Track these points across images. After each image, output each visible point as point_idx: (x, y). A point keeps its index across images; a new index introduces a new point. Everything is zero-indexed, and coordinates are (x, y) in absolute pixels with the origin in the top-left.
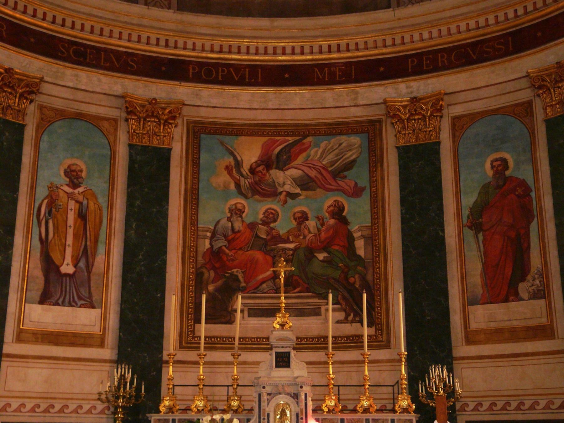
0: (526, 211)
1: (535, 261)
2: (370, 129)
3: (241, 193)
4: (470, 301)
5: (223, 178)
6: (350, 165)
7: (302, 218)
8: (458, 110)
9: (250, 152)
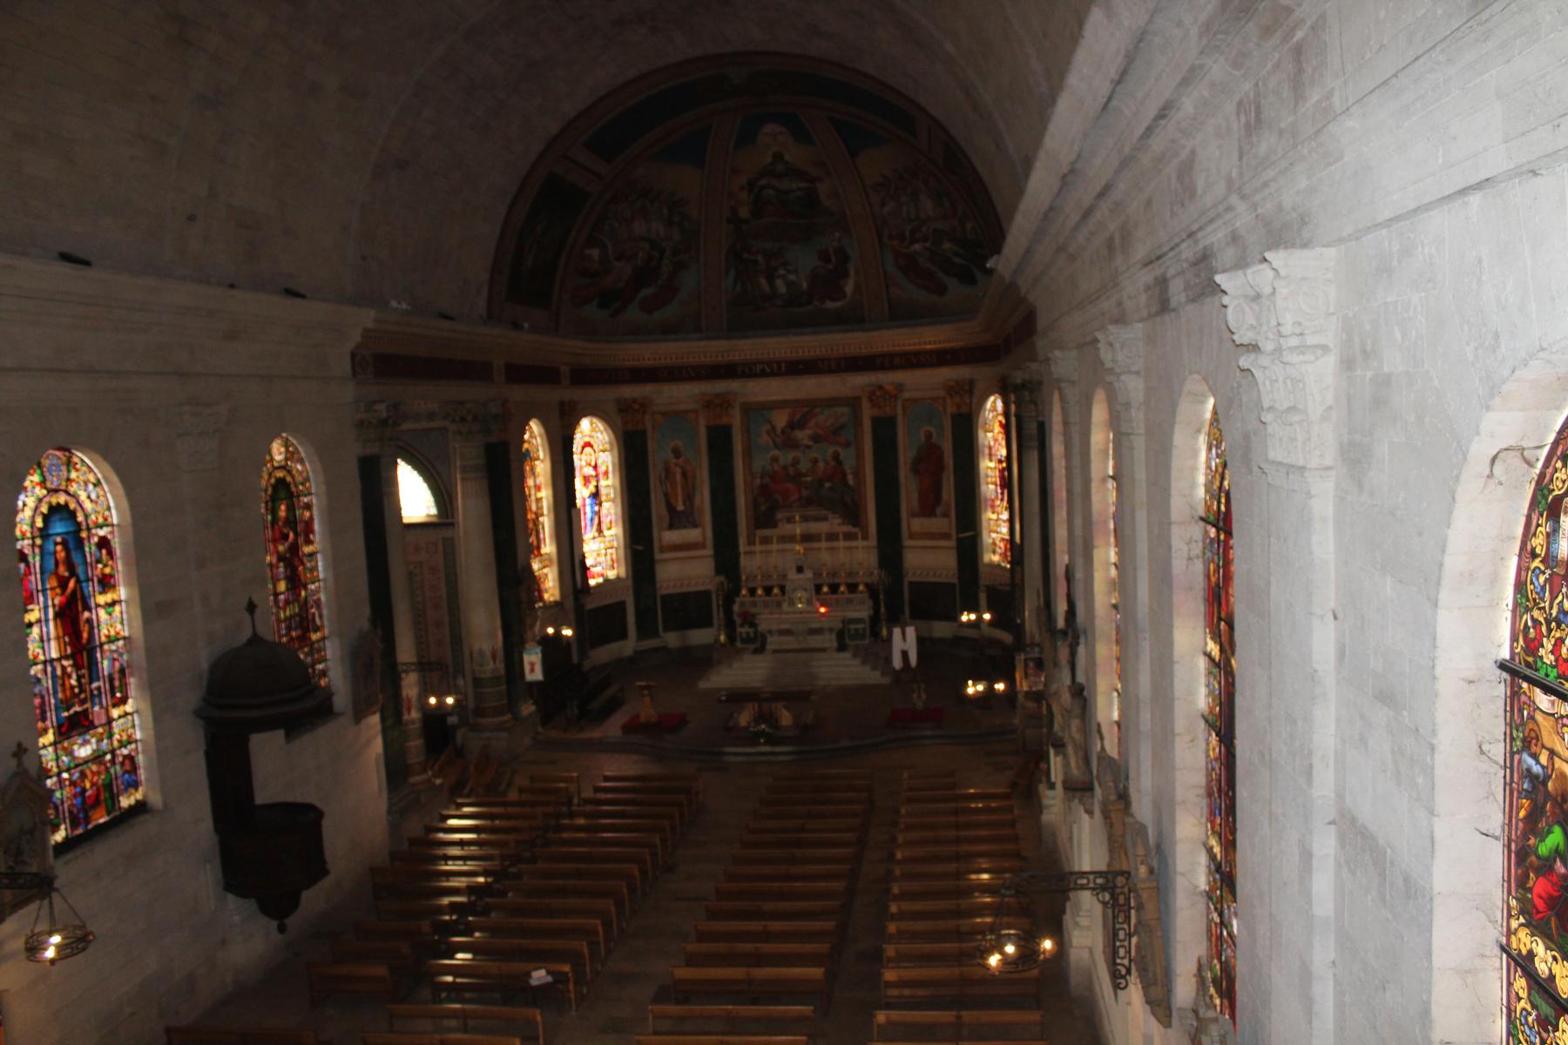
0: (941, 467)
1: (945, 496)
2: (853, 403)
3: (776, 447)
4: (913, 515)
5: (764, 439)
6: (842, 427)
7: (815, 461)
8: (906, 395)
9: (781, 420)
